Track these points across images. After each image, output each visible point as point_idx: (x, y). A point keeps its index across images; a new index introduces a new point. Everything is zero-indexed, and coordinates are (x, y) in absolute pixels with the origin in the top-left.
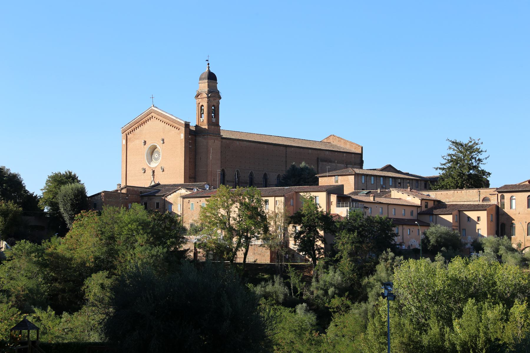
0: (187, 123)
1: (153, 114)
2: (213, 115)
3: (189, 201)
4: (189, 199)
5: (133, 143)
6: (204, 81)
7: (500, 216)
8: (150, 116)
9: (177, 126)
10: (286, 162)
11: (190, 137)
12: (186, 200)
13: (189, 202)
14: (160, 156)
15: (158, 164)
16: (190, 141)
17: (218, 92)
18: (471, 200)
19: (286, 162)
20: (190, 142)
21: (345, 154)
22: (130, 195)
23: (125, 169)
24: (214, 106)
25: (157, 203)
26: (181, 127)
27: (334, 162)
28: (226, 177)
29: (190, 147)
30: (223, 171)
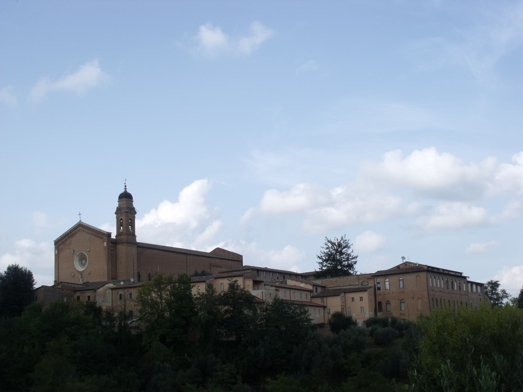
0: (109, 233)
1: (80, 228)
2: (130, 227)
3: (118, 292)
4: (118, 290)
6: (122, 199)
7: (377, 296)
8: (78, 229)
9: (101, 236)
10: (187, 266)
11: (112, 245)
12: (116, 291)
13: (117, 293)
14: (86, 262)
15: (85, 268)
16: (112, 248)
17: (134, 209)
18: (352, 284)
19: (187, 266)
20: (112, 249)
21: (230, 261)
22: (65, 290)
23: (58, 274)
24: (130, 219)
25: (88, 296)
26: (104, 237)
27: (223, 268)
28: (141, 278)
29: (111, 253)
30: (139, 273)
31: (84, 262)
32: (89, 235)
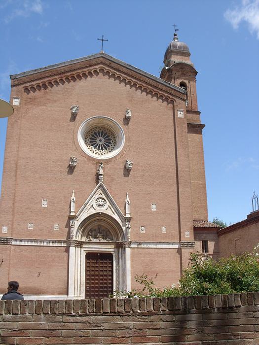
5: (44, 107)
31: (101, 141)
32: (128, 86)
